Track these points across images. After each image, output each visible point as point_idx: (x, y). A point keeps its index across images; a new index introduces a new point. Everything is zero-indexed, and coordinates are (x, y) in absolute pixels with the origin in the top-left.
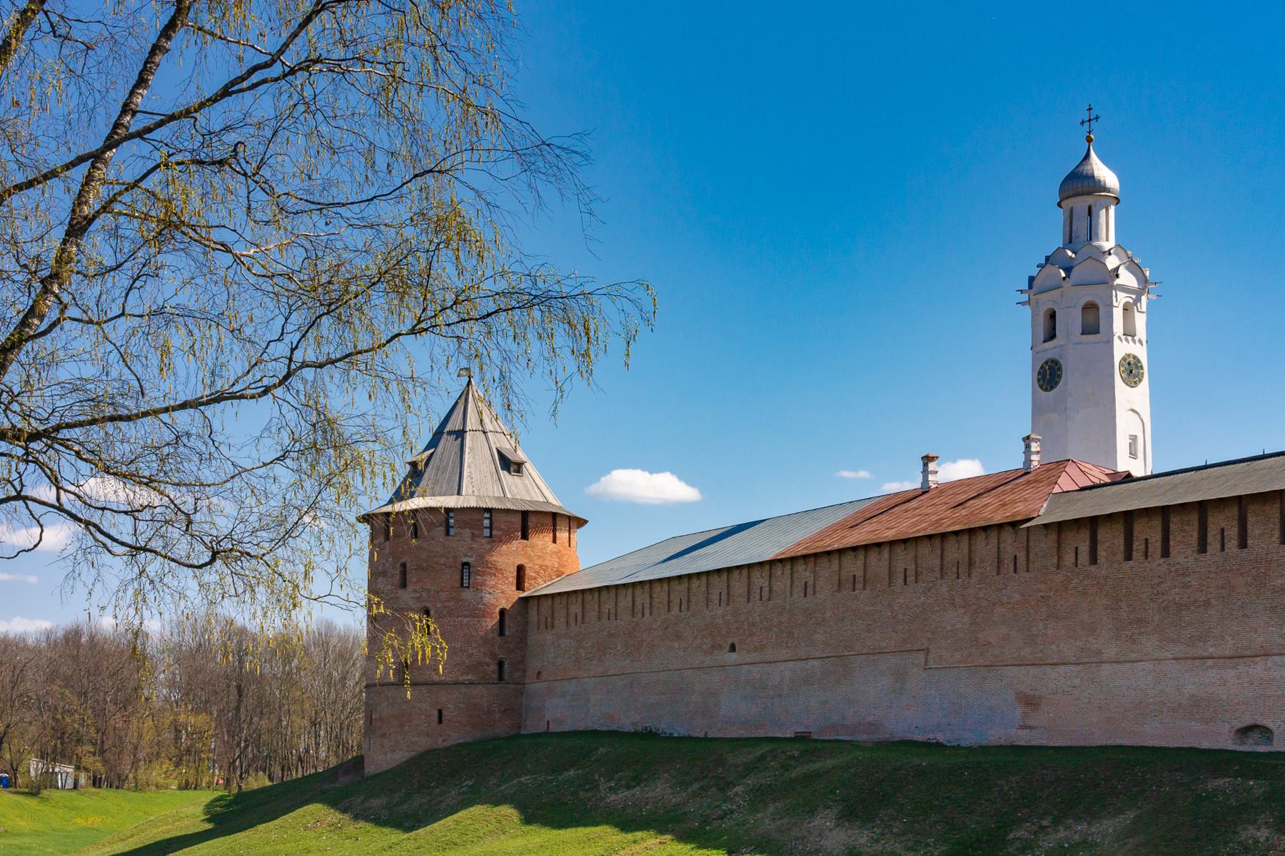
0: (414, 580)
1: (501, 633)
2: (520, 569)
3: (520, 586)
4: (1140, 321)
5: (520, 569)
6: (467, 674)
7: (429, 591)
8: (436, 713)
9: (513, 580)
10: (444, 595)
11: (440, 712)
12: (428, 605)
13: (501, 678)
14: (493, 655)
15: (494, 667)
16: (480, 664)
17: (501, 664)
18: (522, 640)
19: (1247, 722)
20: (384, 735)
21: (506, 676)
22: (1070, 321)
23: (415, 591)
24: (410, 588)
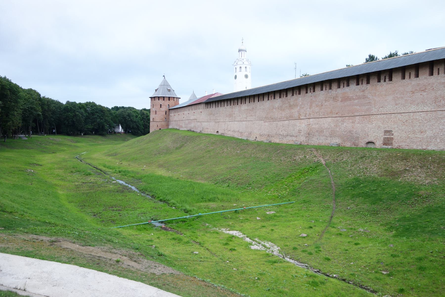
4: (248, 69)
18: (169, 115)
22: (238, 69)
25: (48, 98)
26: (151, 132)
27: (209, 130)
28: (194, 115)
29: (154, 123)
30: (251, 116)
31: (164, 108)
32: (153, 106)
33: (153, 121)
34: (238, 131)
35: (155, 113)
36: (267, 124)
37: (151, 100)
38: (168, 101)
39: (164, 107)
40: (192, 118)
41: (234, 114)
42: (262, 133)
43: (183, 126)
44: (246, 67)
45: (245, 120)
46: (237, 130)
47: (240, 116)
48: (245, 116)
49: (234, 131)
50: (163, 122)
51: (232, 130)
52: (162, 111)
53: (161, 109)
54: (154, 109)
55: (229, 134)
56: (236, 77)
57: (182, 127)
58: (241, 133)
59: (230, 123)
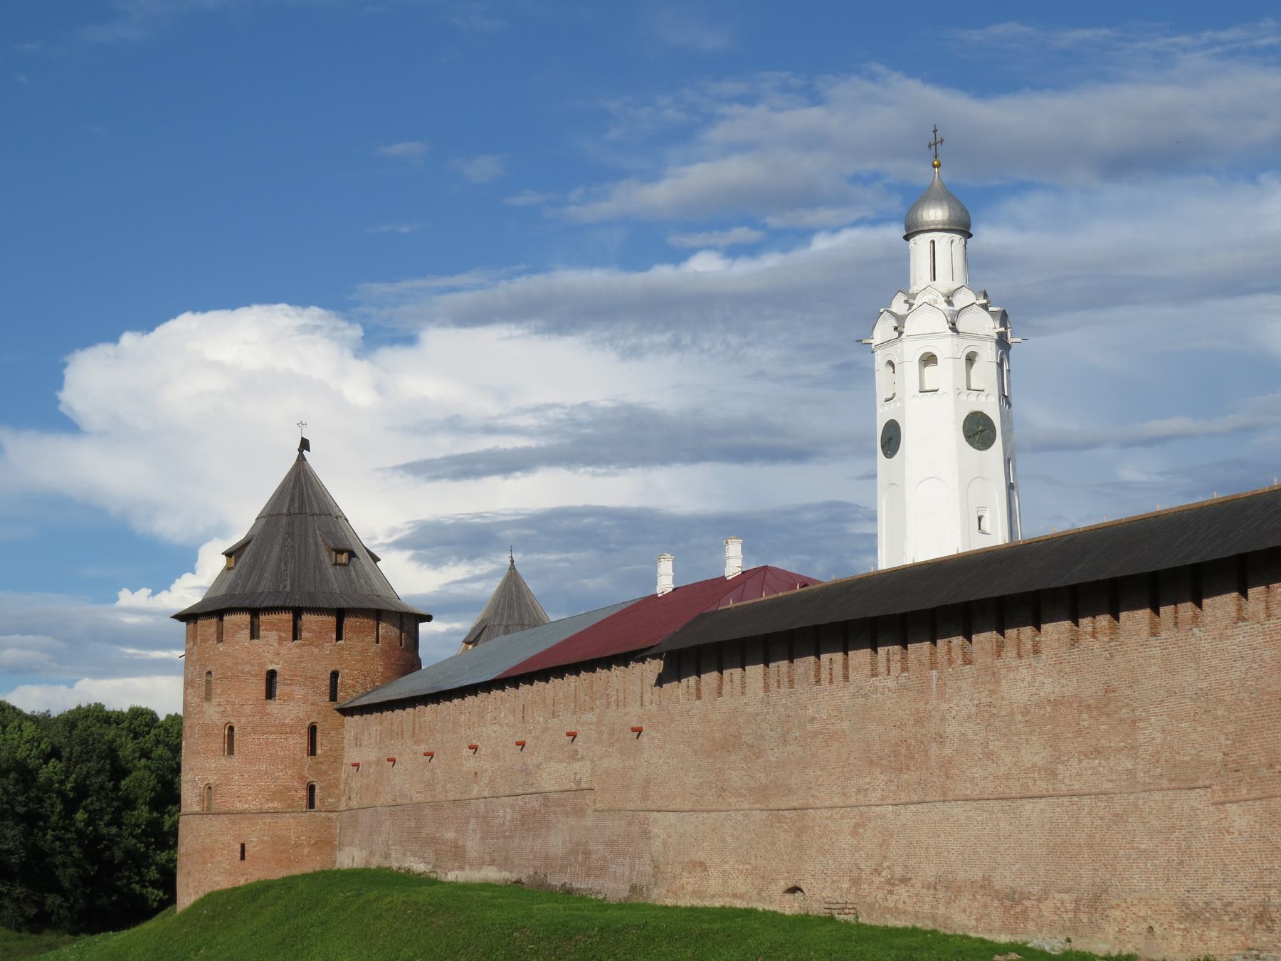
0: (219, 691)
1: (312, 752)
2: (335, 675)
3: (333, 697)
5: (335, 675)
6: (272, 801)
7: (233, 704)
8: (238, 847)
9: (325, 687)
10: (248, 709)
11: (243, 846)
12: (233, 721)
13: (311, 804)
14: (302, 778)
15: (303, 793)
16: (288, 789)
17: (311, 789)
18: (336, 758)
19: (790, 885)
20: (189, 873)
21: (317, 803)
23: (219, 705)
24: (215, 701)
25: (79, 708)
26: (186, 897)
27: (714, 881)
28: (574, 756)
29: (217, 824)
30: (1098, 752)
31: (297, 705)
32: (202, 682)
33: (207, 812)
34: (986, 885)
35: (219, 743)
36: (1240, 818)
37: (192, 637)
38: (329, 645)
39: (299, 692)
40: (554, 775)
41: (941, 739)
42: (1199, 899)
43: (473, 845)
44: (970, 359)
45: (1041, 786)
46: (977, 874)
47: (990, 755)
48: (1034, 753)
49: (945, 885)
50: (288, 820)
51: (930, 871)
52: (282, 729)
53: (274, 707)
54: (213, 714)
55: (897, 912)
56: (892, 439)
57: (458, 855)
58: (1012, 898)
59: (908, 813)
